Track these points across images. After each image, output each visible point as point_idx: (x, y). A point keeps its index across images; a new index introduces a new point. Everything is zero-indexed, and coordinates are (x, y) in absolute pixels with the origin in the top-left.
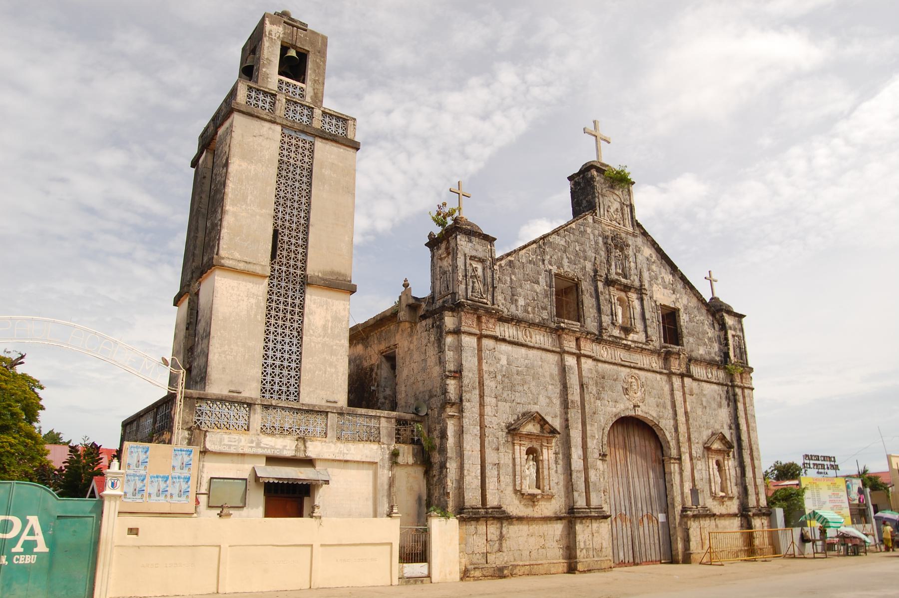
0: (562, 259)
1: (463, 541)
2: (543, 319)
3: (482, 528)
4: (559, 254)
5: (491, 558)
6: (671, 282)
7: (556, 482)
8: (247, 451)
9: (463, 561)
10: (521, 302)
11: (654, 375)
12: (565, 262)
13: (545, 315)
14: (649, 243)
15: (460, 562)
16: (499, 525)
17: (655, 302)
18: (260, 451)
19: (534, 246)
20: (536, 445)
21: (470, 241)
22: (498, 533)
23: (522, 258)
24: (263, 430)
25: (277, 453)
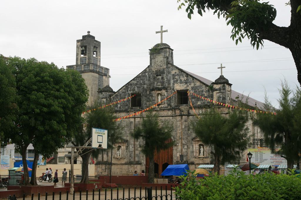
0: (135, 87)
1: (96, 169)
2: (126, 109)
3: (101, 166)
4: (134, 87)
5: (103, 173)
6: (185, 80)
7: (127, 154)
8: (64, 151)
9: (96, 174)
10: (119, 106)
11: (169, 117)
12: (136, 89)
13: (127, 107)
14: (175, 68)
15: (95, 174)
16: (105, 165)
17: (174, 90)
18: (66, 151)
19: (125, 87)
20: (120, 145)
21: (102, 94)
22: (105, 167)
23: (120, 92)
24: (67, 147)
25: (69, 151)
